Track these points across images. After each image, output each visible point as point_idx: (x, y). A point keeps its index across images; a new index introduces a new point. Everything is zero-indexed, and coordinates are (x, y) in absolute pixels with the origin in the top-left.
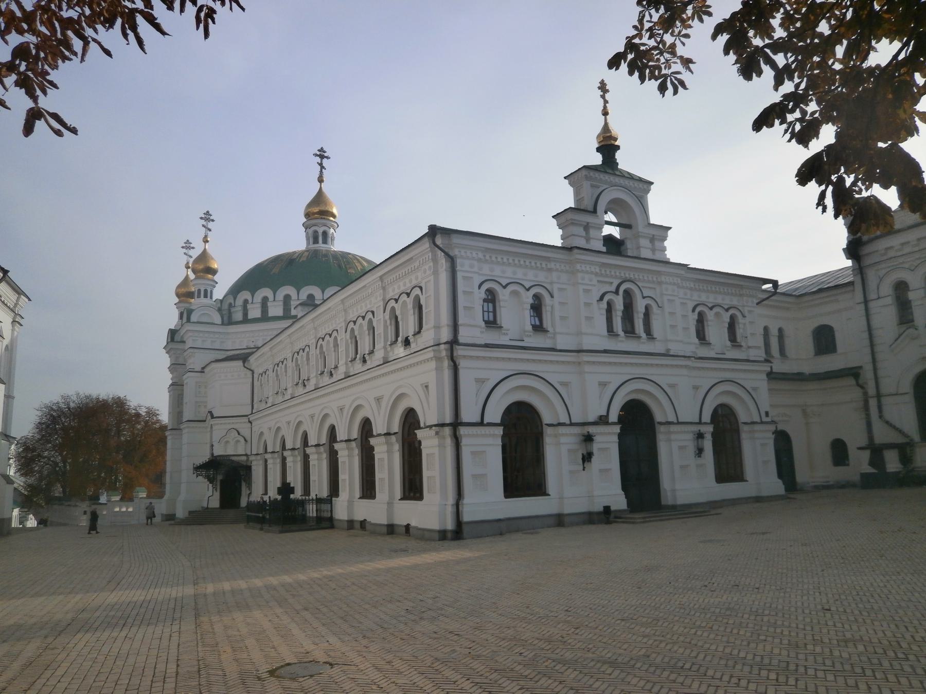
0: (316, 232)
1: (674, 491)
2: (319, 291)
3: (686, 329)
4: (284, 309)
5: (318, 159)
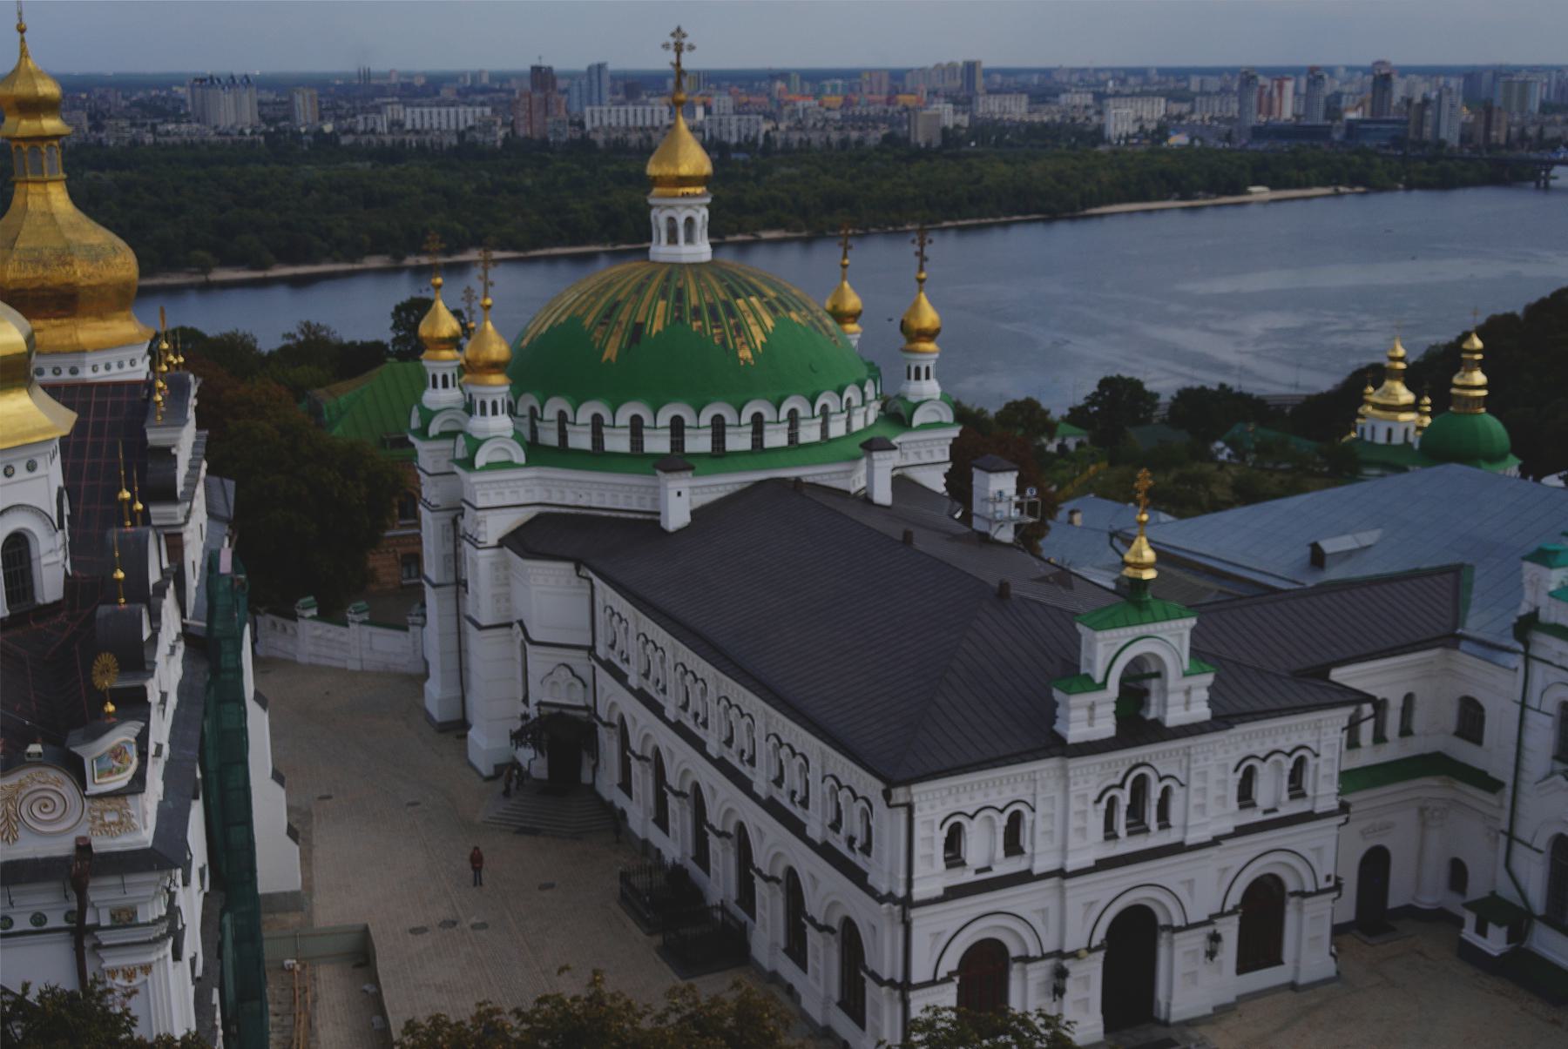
0: (671, 220)
1: (1169, 1005)
2: (693, 414)
3: (1222, 799)
4: (632, 442)
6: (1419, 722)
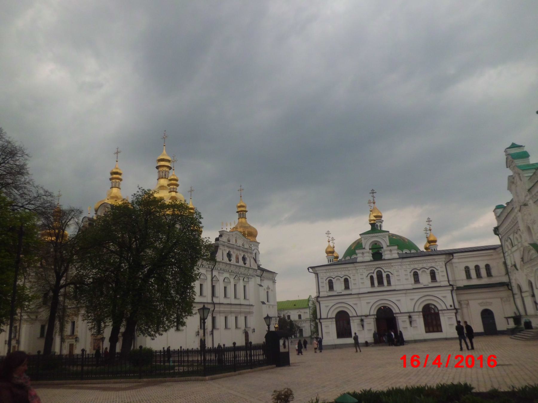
5: (372, 195)
6: (494, 272)
